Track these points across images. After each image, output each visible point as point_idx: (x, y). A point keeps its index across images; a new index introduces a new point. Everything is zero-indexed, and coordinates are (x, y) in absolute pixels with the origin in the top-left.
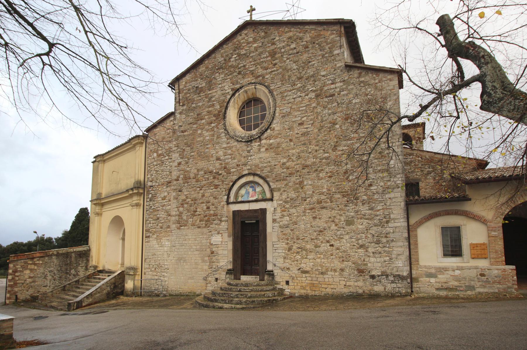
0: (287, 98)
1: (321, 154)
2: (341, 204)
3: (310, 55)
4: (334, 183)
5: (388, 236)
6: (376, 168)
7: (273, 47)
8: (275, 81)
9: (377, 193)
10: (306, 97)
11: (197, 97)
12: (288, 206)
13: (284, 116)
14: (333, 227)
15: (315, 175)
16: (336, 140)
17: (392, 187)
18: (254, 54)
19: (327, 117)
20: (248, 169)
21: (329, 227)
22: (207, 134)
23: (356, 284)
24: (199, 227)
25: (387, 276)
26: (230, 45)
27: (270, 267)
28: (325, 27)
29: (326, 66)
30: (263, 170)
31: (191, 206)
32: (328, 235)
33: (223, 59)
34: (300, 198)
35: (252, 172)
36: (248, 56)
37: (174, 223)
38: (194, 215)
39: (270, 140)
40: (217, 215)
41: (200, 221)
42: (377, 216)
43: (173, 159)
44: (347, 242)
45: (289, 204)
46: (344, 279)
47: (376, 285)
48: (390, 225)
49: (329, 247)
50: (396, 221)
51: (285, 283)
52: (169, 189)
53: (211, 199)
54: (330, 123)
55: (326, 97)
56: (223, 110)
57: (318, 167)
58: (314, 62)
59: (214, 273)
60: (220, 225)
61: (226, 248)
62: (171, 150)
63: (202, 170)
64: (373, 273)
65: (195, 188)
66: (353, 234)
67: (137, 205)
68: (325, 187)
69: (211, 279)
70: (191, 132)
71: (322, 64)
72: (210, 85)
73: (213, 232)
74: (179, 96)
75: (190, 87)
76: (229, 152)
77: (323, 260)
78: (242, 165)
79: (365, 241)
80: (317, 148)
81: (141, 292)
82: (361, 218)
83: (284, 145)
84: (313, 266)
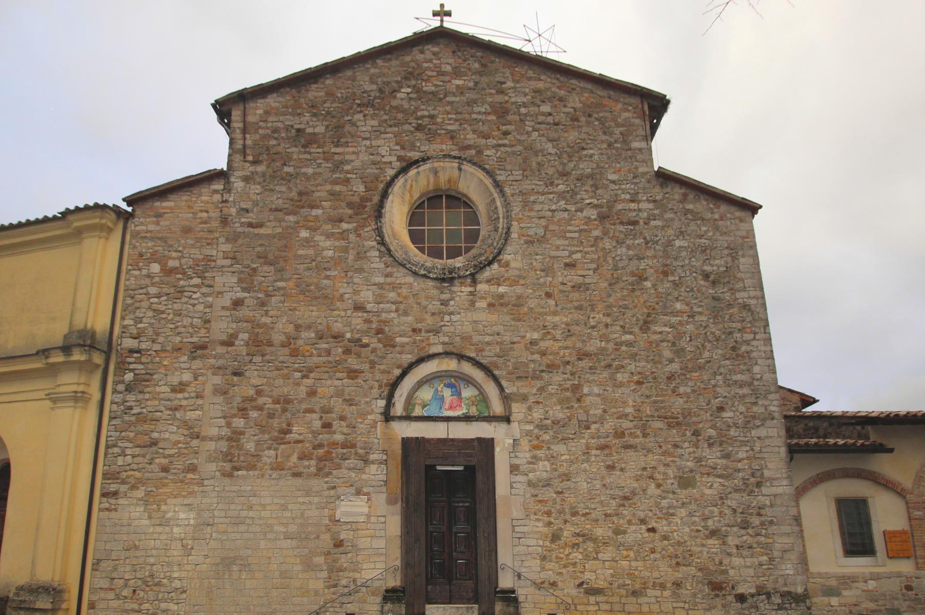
0: (537, 207)
1: (616, 333)
2: (666, 442)
3: (583, 136)
4: (647, 397)
5: (763, 512)
7: (500, 98)
8: (508, 167)
10: (579, 213)
11: (300, 152)
12: (546, 437)
13: (532, 242)
14: (652, 489)
15: (605, 374)
16: (645, 311)
17: (762, 417)
18: (458, 99)
19: (626, 262)
20: (443, 343)
21: (644, 491)
22: (328, 243)
24: (297, 475)
25: (768, 595)
26: (395, 63)
28: (612, 93)
29: (618, 165)
30: (483, 350)
31: (271, 416)
32: (643, 506)
33: (374, 87)
35: (454, 351)
36: (440, 100)
37: (210, 460)
38: (279, 441)
39: (499, 285)
40: (353, 446)
41: (300, 458)
42: (739, 470)
43: (217, 289)
44: (684, 524)
45: (551, 433)
46: (682, 605)
48: (765, 490)
49: (646, 535)
50: (775, 483)
52: (197, 364)
53: (338, 405)
54: (633, 274)
55: (622, 223)
56: (376, 199)
58: (592, 152)
59: (345, 599)
60: (362, 470)
61: (382, 533)
62: (213, 264)
63: (309, 327)
64: (741, 590)
65: (286, 371)
66: (693, 507)
67: (79, 398)
70: (279, 230)
71: (609, 158)
72: (338, 134)
73: (340, 491)
74: (245, 139)
75: (279, 125)
77: (634, 564)
78: (428, 331)
79: (720, 521)
80: (609, 320)
82: (708, 474)
83: (532, 303)
84: (612, 576)
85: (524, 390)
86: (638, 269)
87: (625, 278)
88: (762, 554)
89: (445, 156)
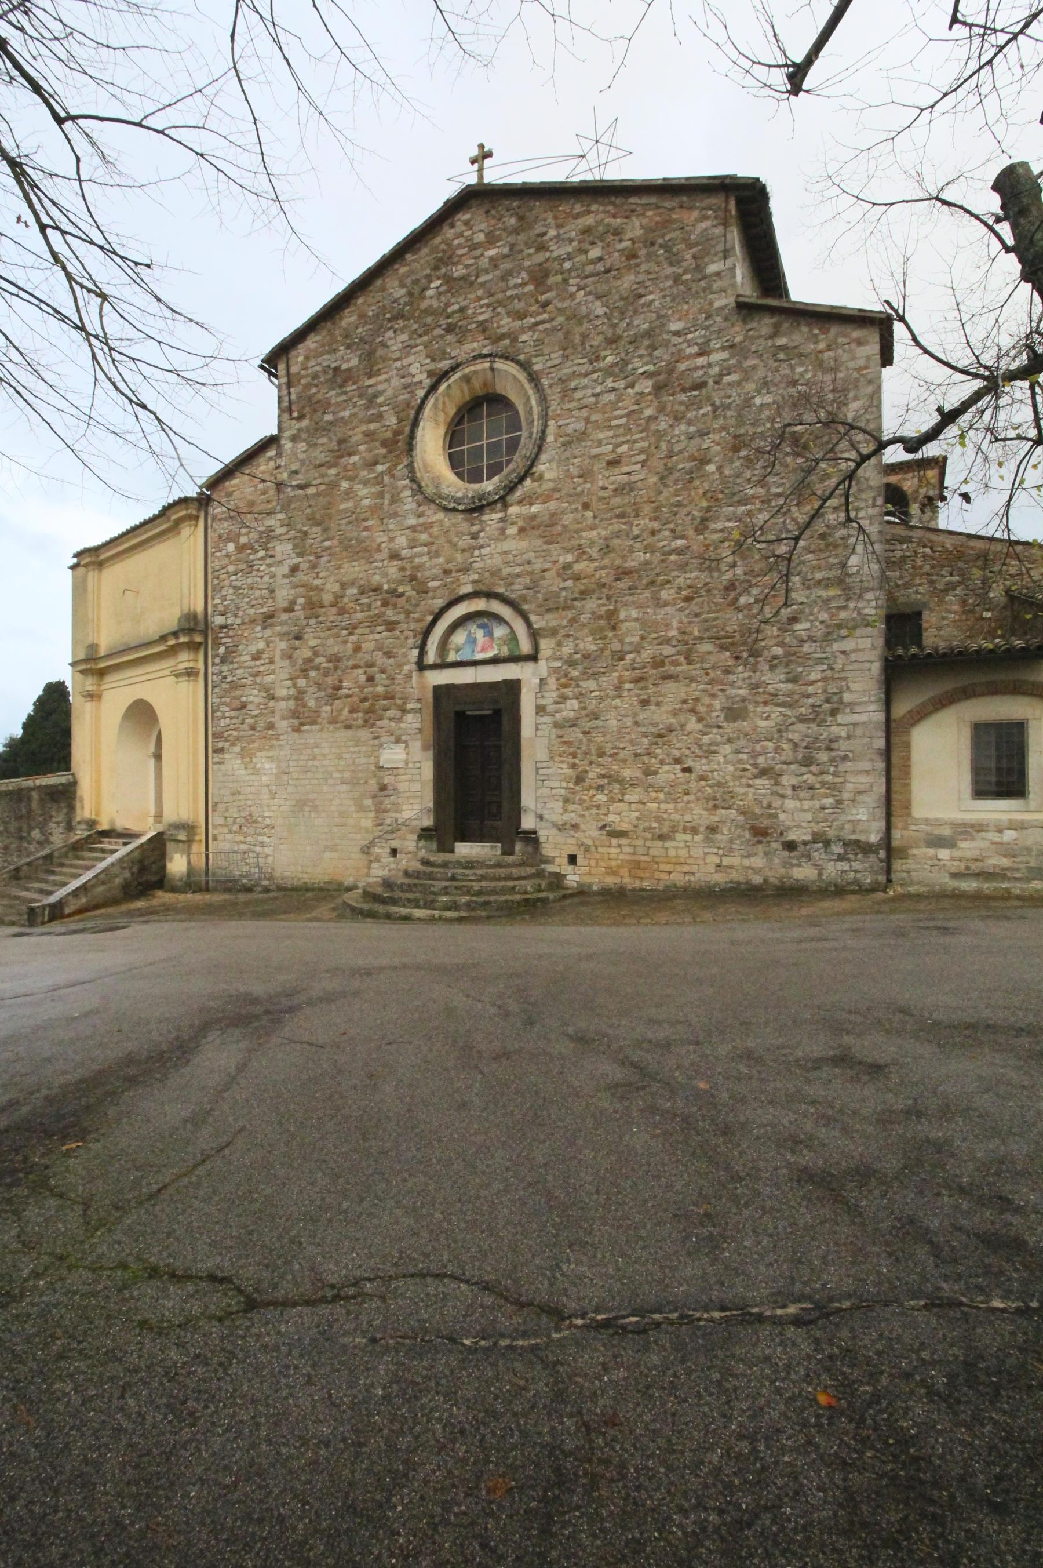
0: (578, 395)
1: (664, 540)
2: (713, 668)
3: (641, 277)
4: (697, 615)
5: (835, 745)
6: (809, 576)
7: (540, 257)
8: (546, 351)
9: (810, 638)
10: (630, 390)
11: (338, 395)
12: (575, 673)
13: (570, 443)
14: (693, 724)
15: (647, 594)
16: (705, 504)
17: (851, 624)
18: (489, 277)
20: (474, 582)
23: (746, 862)
24: (348, 727)
26: (425, 251)
27: (527, 823)
28: (685, 199)
29: (686, 307)
30: (512, 584)
31: (326, 674)
32: (679, 745)
33: (403, 291)
34: (608, 653)
35: (484, 588)
36: (472, 283)
37: (283, 718)
38: (333, 698)
39: (531, 504)
40: (393, 698)
41: (351, 712)
42: (808, 696)
43: (279, 557)
44: (726, 762)
45: (580, 667)
47: (799, 865)
48: (840, 718)
49: (680, 775)
50: (858, 709)
51: (565, 860)
52: (268, 632)
53: (380, 659)
55: (684, 390)
56: (407, 429)
57: (658, 575)
58: (651, 297)
59: (389, 836)
60: (400, 720)
64: (792, 836)
65: (335, 630)
66: (742, 742)
67: (190, 673)
68: (675, 624)
69: (382, 851)
71: (673, 300)
72: (371, 363)
73: (383, 739)
74: (289, 393)
75: (318, 368)
76: (424, 537)
77: (663, 806)
78: (459, 571)
79: (773, 758)
80: (656, 525)
81: (207, 882)
82: (765, 703)
83: (568, 519)
84: (638, 818)
85: (554, 623)
86: (699, 450)
87: (680, 466)
88: (827, 796)
89: (475, 358)
